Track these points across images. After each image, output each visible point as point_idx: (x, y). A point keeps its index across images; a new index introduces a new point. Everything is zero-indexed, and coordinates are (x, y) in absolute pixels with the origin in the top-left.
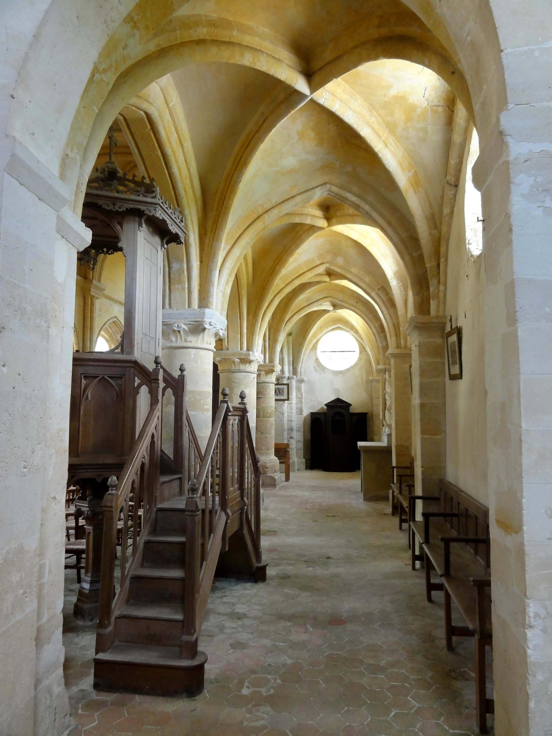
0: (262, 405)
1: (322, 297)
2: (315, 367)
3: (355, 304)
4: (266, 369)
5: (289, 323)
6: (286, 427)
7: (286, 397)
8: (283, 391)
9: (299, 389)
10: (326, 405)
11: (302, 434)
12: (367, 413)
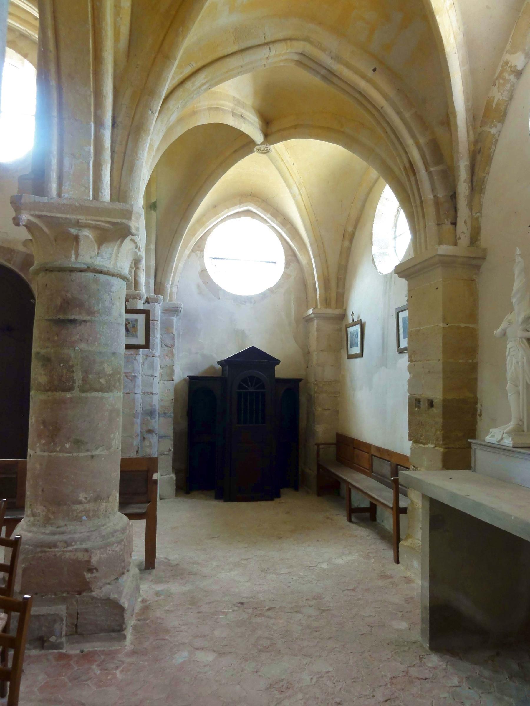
0: (83, 346)
1: (281, 36)
2: (198, 286)
3: (370, 73)
4: (102, 221)
5: (179, 93)
6: (139, 408)
7: (141, 341)
9: (167, 328)
10: (219, 363)
11: (170, 420)
12: (300, 380)
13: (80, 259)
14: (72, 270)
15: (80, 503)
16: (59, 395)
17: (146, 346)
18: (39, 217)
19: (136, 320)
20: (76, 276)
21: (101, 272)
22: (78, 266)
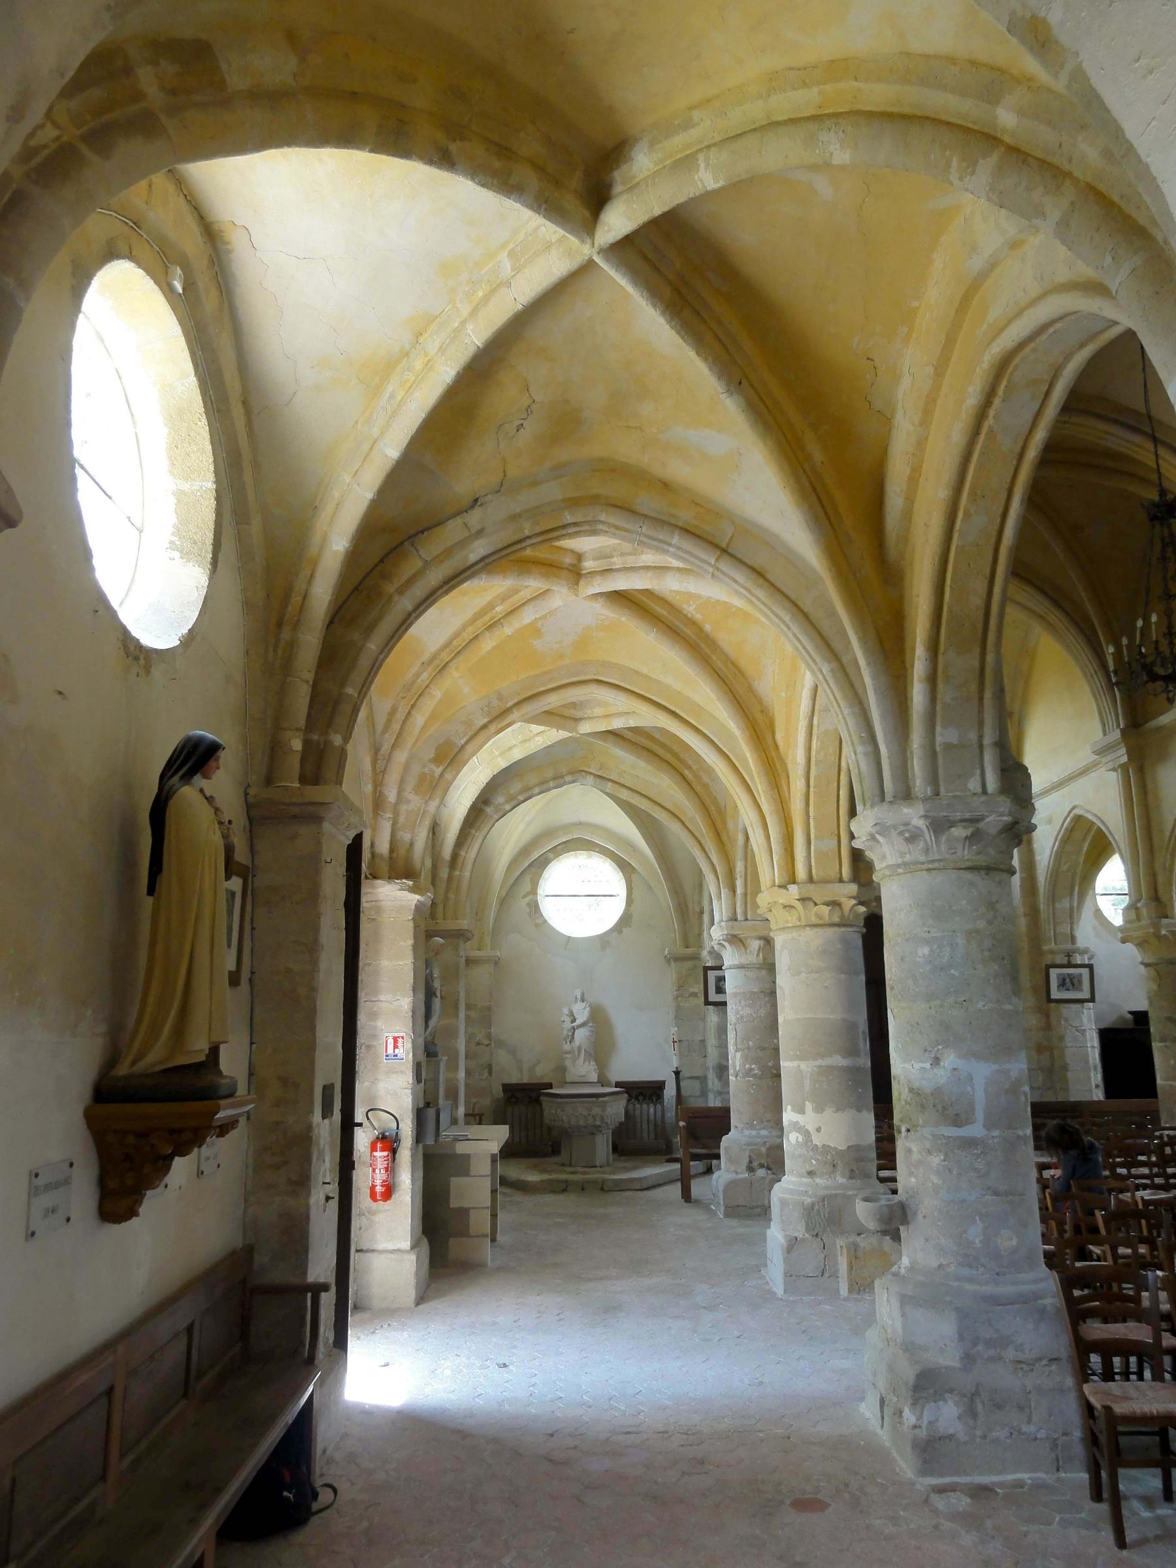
2: (1095, 928)
7: (1086, 994)
8: (1080, 982)
10: (1130, 1013)
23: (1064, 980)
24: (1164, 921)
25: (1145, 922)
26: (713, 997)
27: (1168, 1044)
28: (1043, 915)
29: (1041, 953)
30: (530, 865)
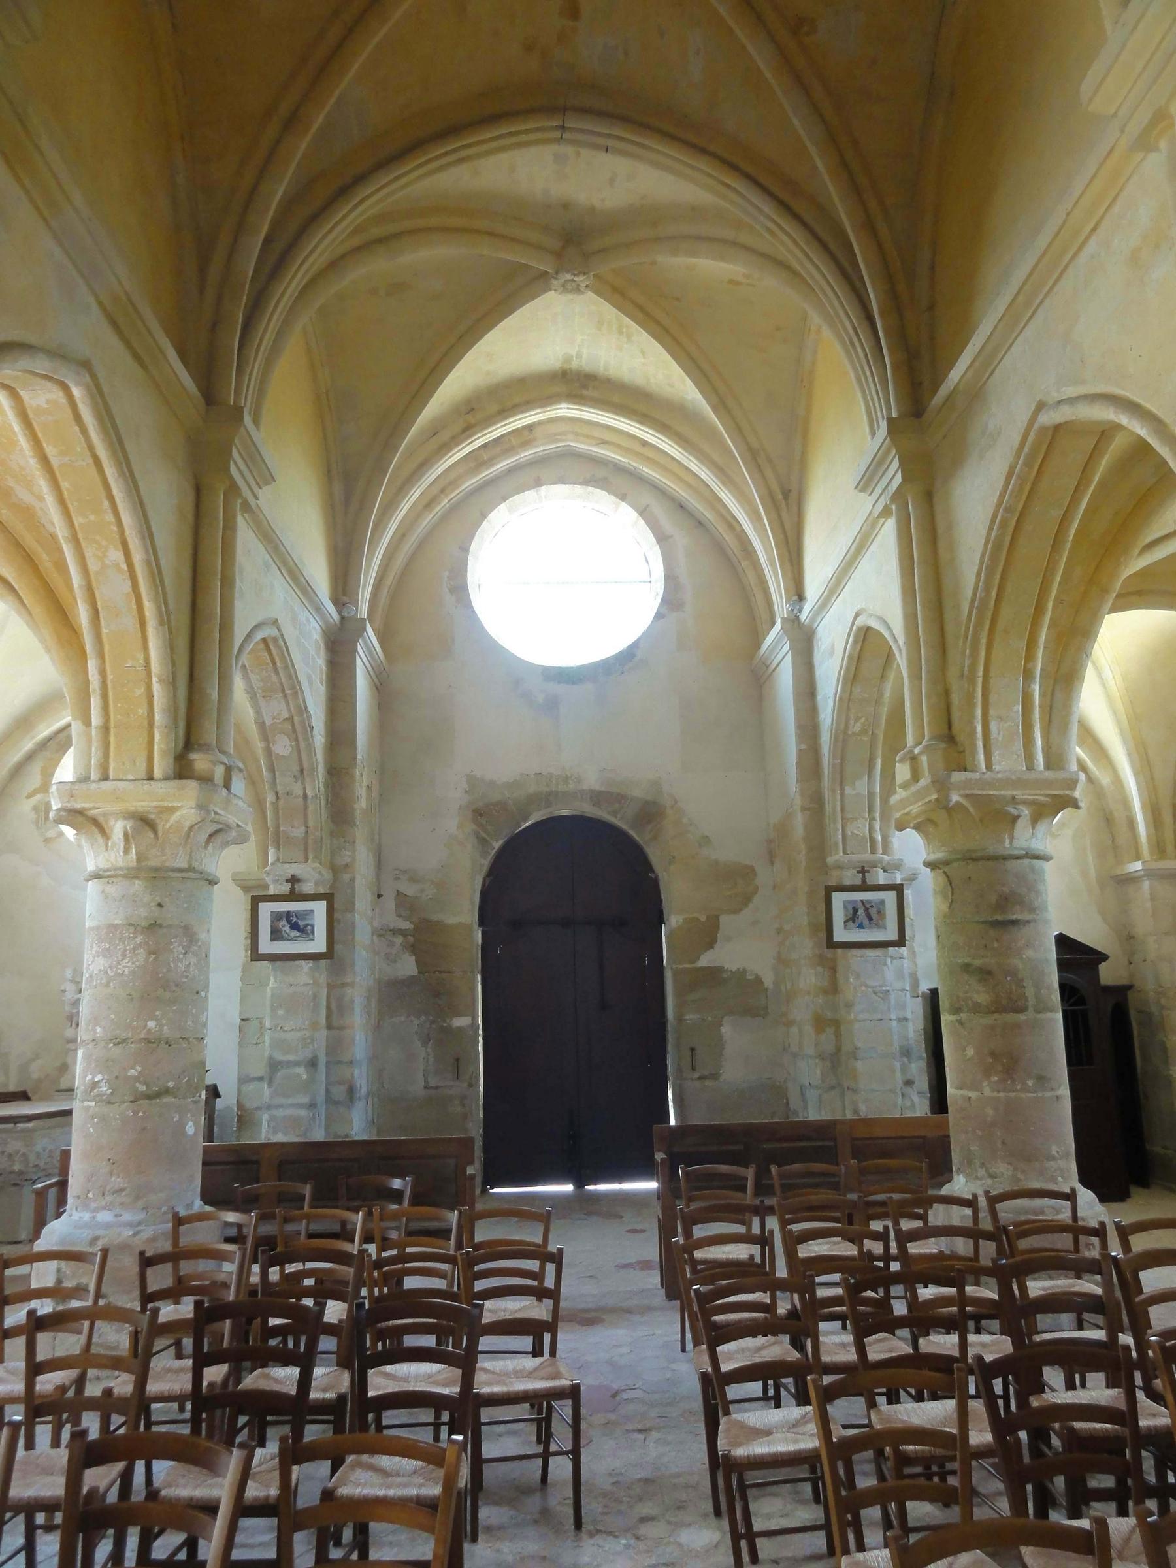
0: (1030, 953)
7: (891, 934)
8: (881, 913)
12: (1130, 987)
13: (1016, 843)
14: (1005, 858)
15: (1054, 1158)
16: (1010, 1017)
17: (901, 942)
18: (967, 796)
19: (882, 902)
20: (1011, 864)
21: (1037, 857)
22: (1016, 852)
23: (855, 910)
24: (958, 777)
25: (924, 781)
26: (266, 946)
27: (963, 1016)
28: (828, 809)
29: (825, 869)
30: (43, 745)
